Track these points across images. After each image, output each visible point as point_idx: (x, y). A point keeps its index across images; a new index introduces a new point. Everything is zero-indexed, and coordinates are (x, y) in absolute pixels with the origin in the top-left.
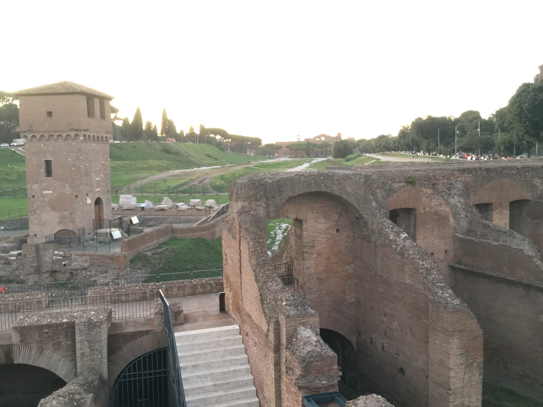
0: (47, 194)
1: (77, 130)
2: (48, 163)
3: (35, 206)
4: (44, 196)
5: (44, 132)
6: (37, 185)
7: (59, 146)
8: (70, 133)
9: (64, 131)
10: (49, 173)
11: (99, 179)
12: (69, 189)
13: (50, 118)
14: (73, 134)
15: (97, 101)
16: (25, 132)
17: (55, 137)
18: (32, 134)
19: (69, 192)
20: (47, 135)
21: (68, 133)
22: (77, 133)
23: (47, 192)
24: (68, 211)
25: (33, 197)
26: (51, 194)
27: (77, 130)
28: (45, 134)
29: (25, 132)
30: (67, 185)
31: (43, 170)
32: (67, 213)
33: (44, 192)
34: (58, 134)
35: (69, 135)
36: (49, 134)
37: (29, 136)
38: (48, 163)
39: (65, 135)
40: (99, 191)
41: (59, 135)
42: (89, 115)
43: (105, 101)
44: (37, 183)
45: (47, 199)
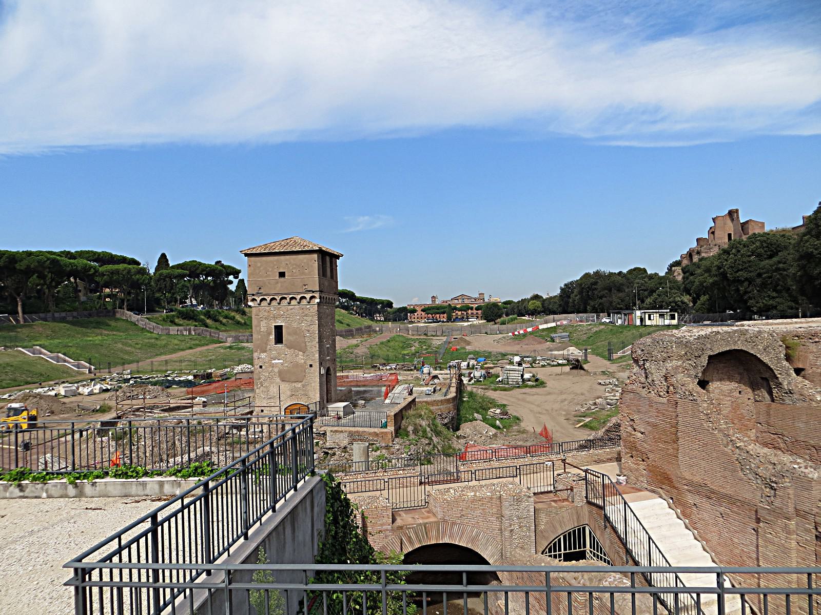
0: (276, 363)
1: (313, 292)
2: (279, 329)
3: (263, 377)
4: (273, 366)
5: (276, 294)
6: (265, 354)
7: (291, 309)
8: (305, 295)
9: (298, 293)
10: (279, 339)
11: (328, 346)
12: (302, 357)
13: (282, 279)
14: (308, 296)
15: (328, 259)
16: (253, 295)
17: (288, 299)
18: (261, 297)
19: (303, 361)
20: (278, 298)
21: (302, 295)
22: (314, 294)
23: (277, 361)
24: (301, 382)
25: (261, 367)
26: (282, 364)
27: (313, 292)
28: (275, 297)
29: (253, 295)
30: (301, 353)
31: (272, 337)
32: (299, 385)
33: (273, 362)
34: (291, 296)
35: (304, 298)
36: (281, 296)
37: (258, 299)
38: (279, 329)
39: (298, 297)
40: (328, 360)
41: (292, 299)
42: (323, 276)
43: (334, 259)
44: (265, 351)
45: (276, 370)
